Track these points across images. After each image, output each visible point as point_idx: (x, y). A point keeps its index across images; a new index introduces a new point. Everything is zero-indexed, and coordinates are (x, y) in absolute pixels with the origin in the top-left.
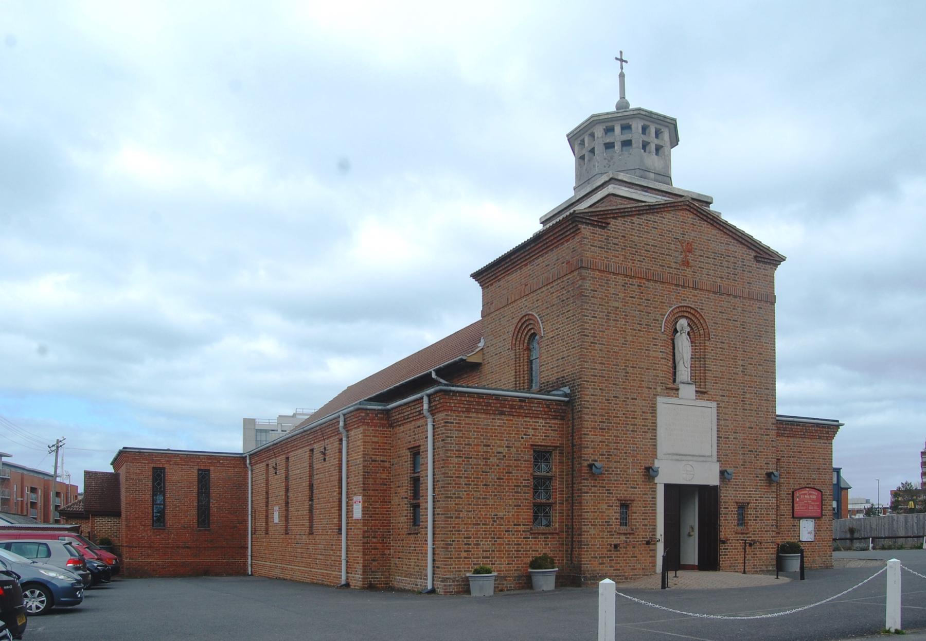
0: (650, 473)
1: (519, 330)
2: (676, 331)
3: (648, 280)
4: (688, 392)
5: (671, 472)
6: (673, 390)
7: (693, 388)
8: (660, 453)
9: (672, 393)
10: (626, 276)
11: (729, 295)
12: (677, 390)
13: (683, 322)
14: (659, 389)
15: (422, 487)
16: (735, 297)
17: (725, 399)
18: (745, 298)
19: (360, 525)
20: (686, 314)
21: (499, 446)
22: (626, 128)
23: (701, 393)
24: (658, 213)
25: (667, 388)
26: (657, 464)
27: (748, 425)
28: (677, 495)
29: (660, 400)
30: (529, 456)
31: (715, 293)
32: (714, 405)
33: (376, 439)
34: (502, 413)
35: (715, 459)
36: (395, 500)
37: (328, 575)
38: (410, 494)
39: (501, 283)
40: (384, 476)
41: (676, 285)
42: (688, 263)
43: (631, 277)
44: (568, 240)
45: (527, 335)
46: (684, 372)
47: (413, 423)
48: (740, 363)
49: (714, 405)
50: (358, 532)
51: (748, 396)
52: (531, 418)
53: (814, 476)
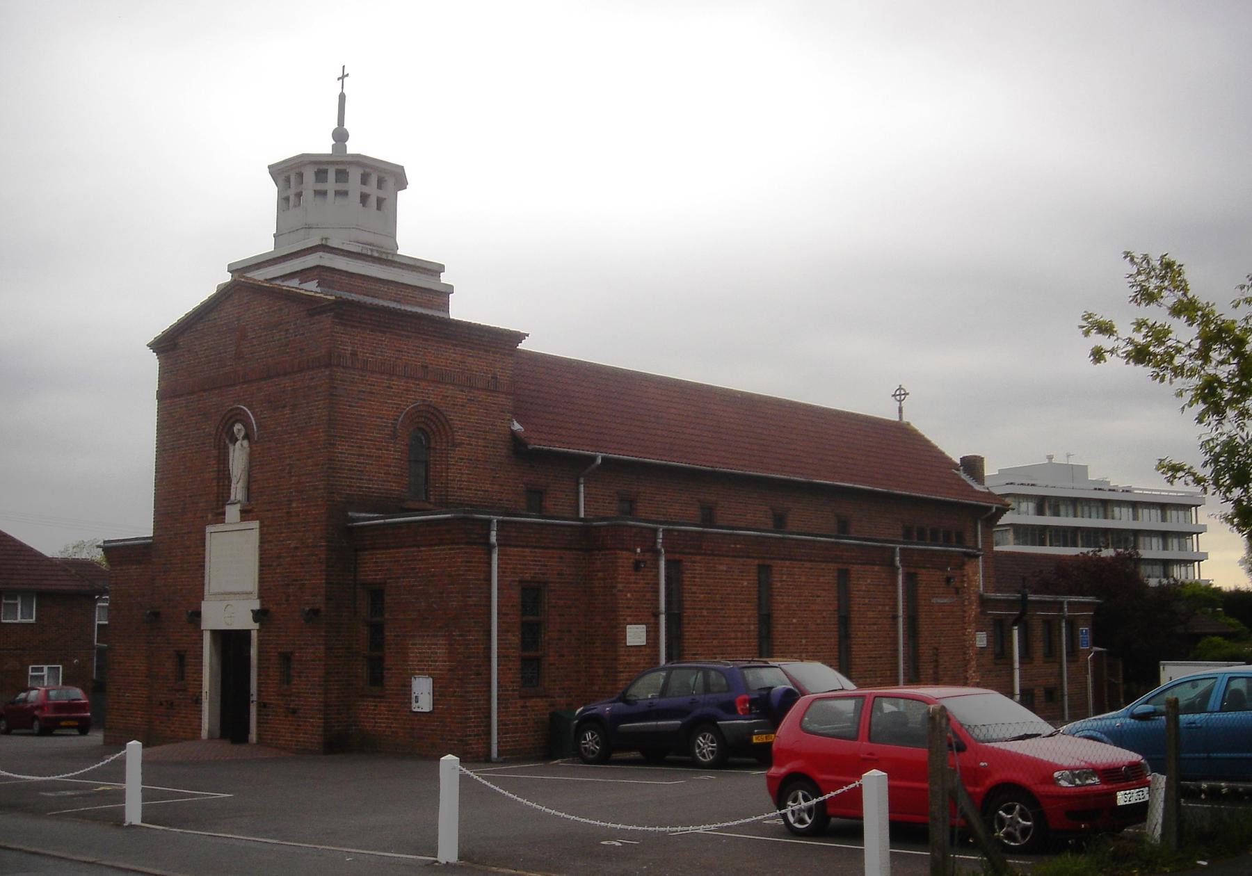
0: (197, 615)
6: (220, 517)
14: (210, 516)
23: (246, 514)
29: (209, 529)
32: (256, 524)
35: (256, 595)
46: (237, 491)
49: (256, 524)
51: (294, 505)
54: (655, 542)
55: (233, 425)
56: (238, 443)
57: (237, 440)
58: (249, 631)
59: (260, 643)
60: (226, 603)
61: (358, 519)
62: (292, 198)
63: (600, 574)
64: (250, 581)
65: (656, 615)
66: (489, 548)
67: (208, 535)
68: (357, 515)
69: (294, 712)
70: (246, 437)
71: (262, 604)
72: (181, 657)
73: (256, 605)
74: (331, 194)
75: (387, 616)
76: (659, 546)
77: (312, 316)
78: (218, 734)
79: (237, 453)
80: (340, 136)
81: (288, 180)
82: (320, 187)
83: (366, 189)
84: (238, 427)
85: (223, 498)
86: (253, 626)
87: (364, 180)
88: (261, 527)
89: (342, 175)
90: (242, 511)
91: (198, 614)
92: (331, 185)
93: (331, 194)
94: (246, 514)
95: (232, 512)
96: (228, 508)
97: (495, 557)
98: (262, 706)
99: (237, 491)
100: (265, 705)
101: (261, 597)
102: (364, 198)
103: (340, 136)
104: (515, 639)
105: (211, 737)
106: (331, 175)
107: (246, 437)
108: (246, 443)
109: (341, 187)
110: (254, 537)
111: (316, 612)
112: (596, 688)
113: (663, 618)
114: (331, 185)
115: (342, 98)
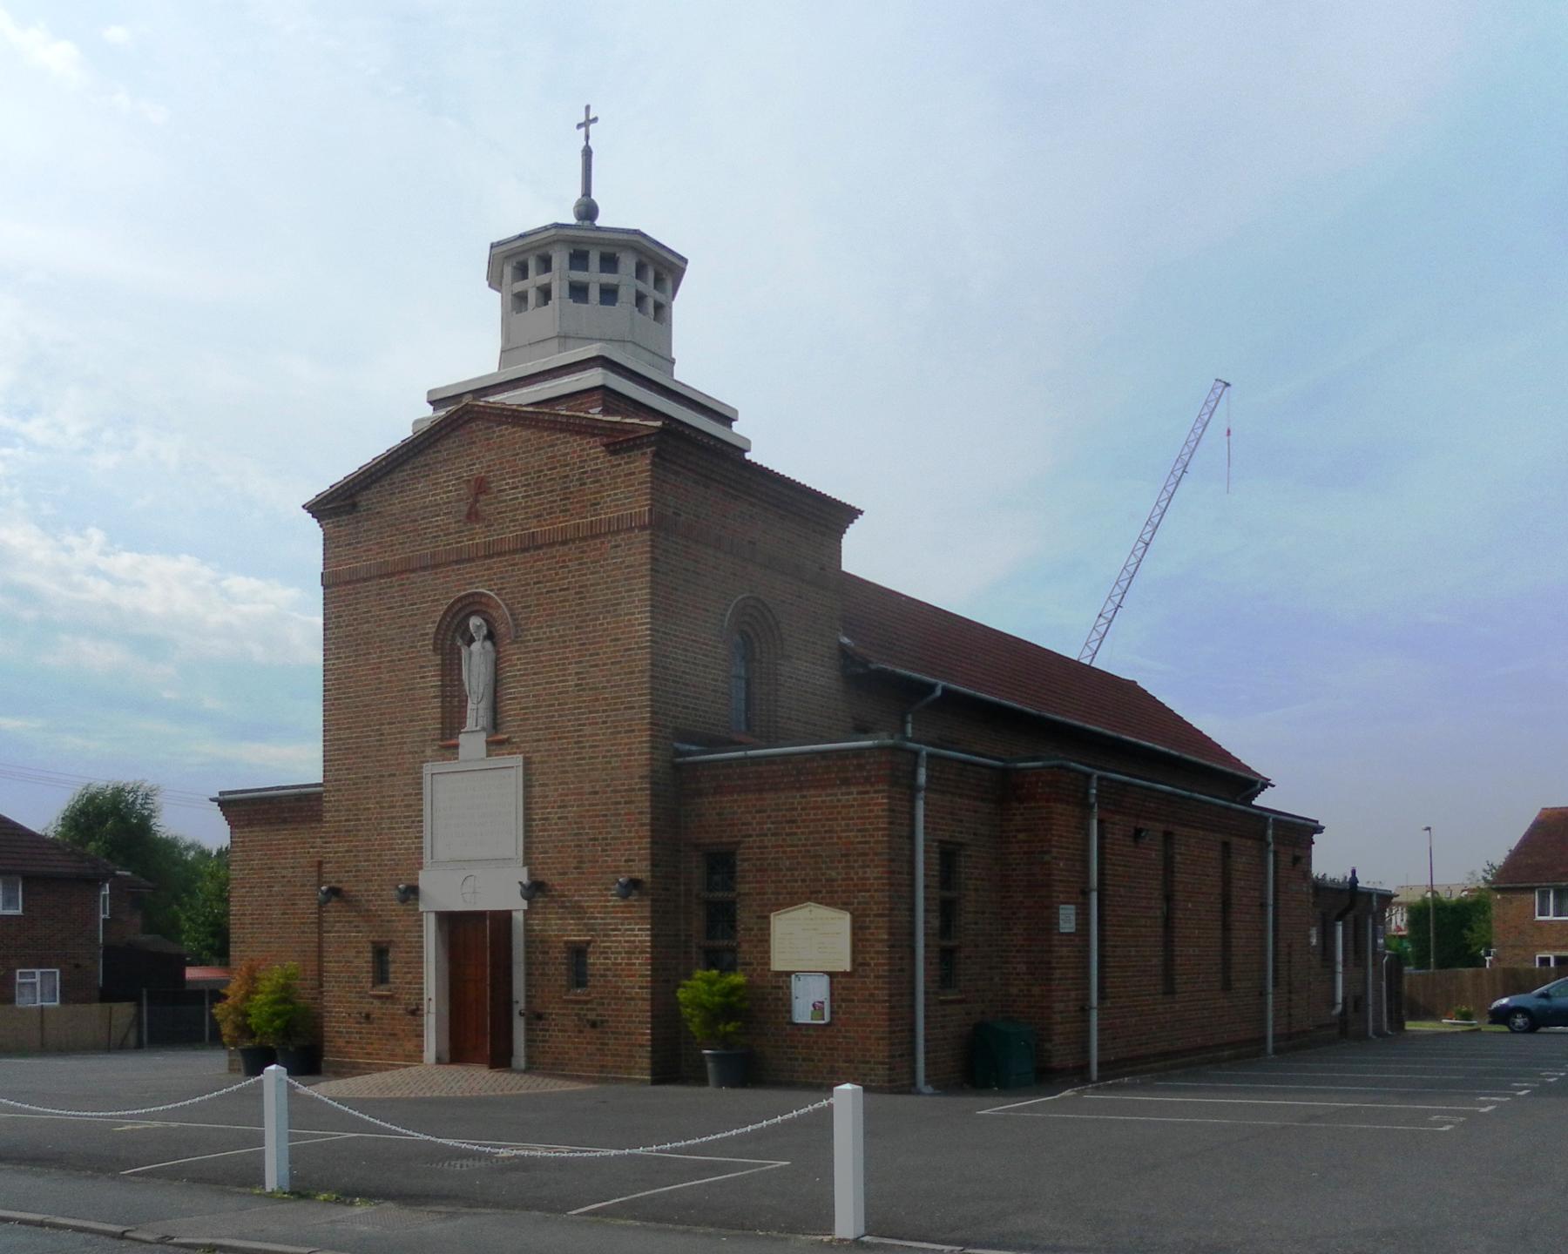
0: (412, 892)
3: (413, 571)
5: (443, 890)
6: (449, 749)
7: (483, 736)
9: (448, 754)
11: (552, 544)
12: (456, 746)
14: (429, 752)
16: (564, 543)
18: (584, 539)
20: (477, 607)
22: (546, 264)
23: (496, 745)
24: (429, 447)
25: (443, 747)
27: (587, 787)
28: (455, 924)
29: (428, 769)
42: (477, 514)
46: (476, 712)
51: (588, 730)
53: (834, 874)
54: (1087, 794)
56: (476, 646)
57: (471, 640)
58: (507, 916)
59: (528, 930)
61: (690, 753)
62: (532, 297)
63: (1021, 836)
64: (512, 842)
65: (1085, 893)
66: (913, 789)
67: (427, 780)
68: (687, 747)
69: (594, 1025)
70: (490, 636)
71: (530, 874)
72: (381, 953)
73: (523, 875)
74: (594, 293)
75: (743, 888)
76: (1093, 800)
78: (447, 1057)
79: (476, 659)
80: (588, 210)
81: (522, 271)
82: (579, 276)
83: (641, 286)
84: (475, 622)
85: (452, 722)
86: (524, 905)
87: (640, 271)
88: (527, 763)
89: (609, 263)
90: (488, 743)
92: (594, 277)
93: (594, 293)
95: (472, 743)
96: (462, 739)
97: (920, 805)
98: (535, 1017)
99: (476, 712)
100: (540, 1017)
101: (528, 860)
102: (640, 299)
103: (588, 210)
104: (936, 923)
105: (439, 1061)
107: (490, 636)
108: (488, 644)
109: (608, 278)
110: (515, 778)
111: (634, 884)
112: (1014, 991)
113: (1094, 896)
114: (594, 277)
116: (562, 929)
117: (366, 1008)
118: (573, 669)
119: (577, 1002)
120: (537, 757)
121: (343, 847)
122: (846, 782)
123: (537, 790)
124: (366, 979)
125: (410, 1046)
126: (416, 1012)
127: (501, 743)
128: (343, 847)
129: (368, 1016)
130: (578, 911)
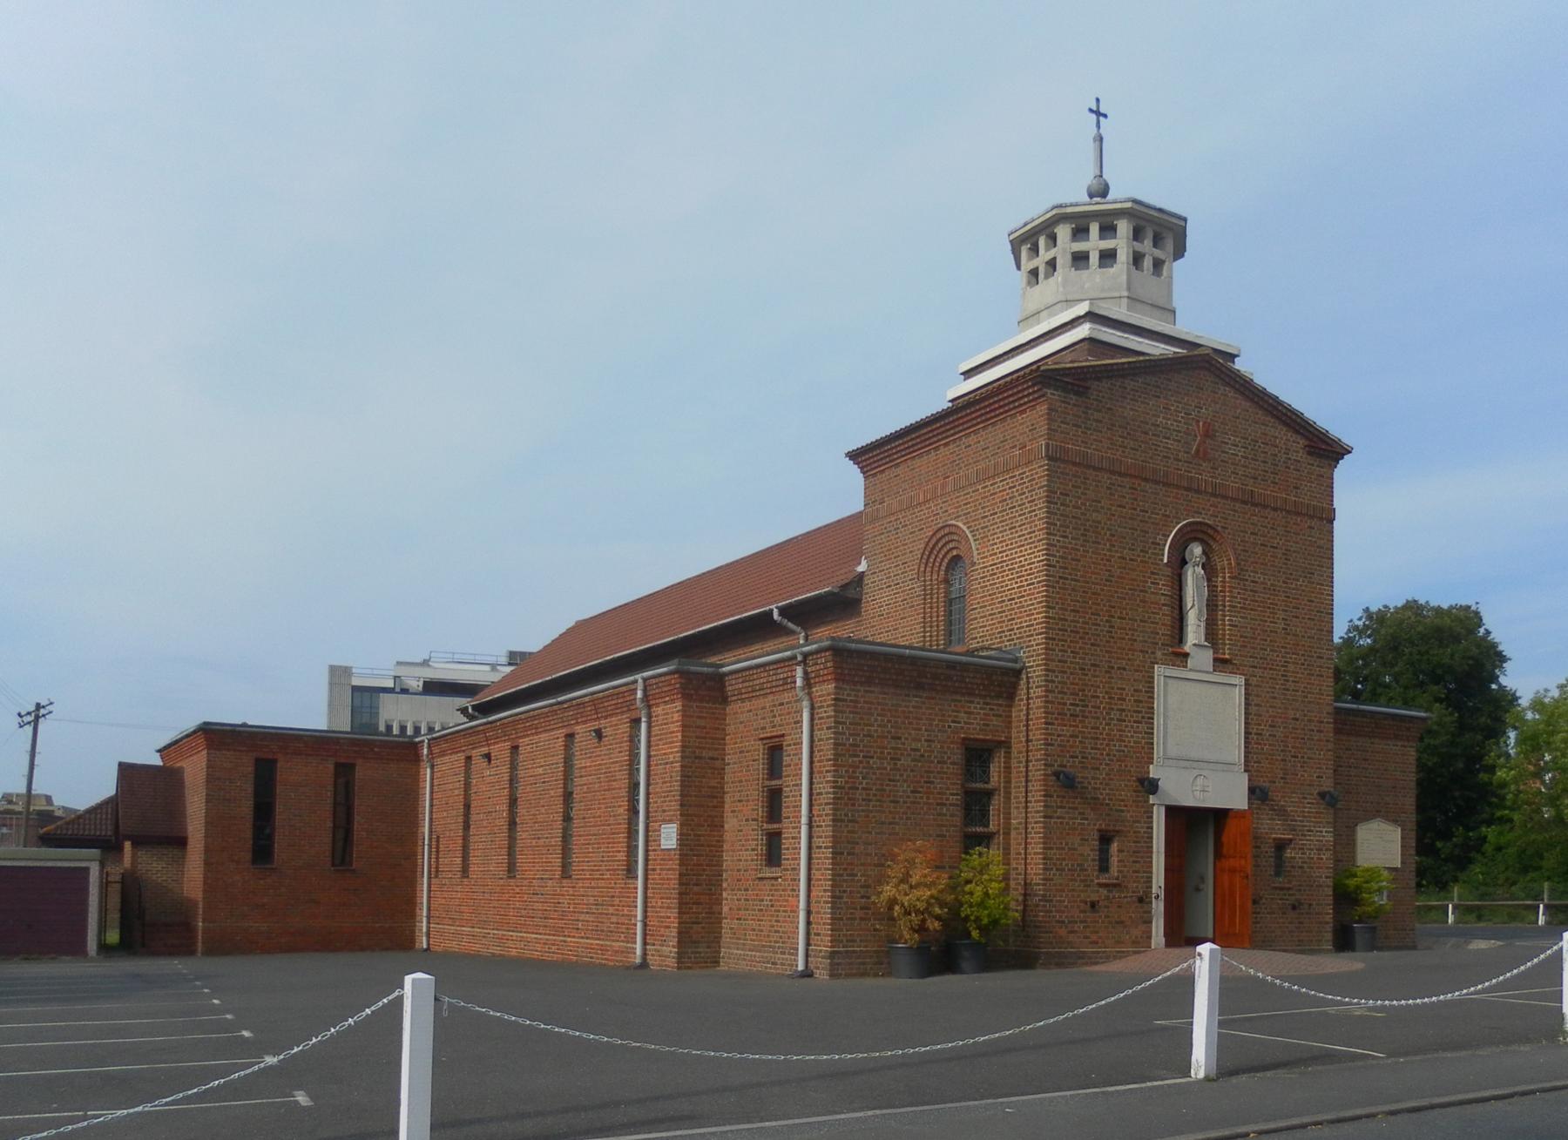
1: (931, 550)
2: (1184, 562)
3: (1146, 480)
4: (1202, 659)
8: (1158, 752)
10: (1113, 472)
11: (1265, 507)
13: (1197, 550)
14: (1159, 654)
15: (787, 802)
16: (1275, 509)
17: (1258, 672)
19: (675, 865)
21: (914, 740)
23: (1221, 663)
26: (1154, 772)
27: (1291, 714)
29: (1159, 671)
30: (957, 755)
31: (1245, 502)
33: (700, 722)
34: (920, 686)
36: (731, 823)
37: (604, 949)
38: (761, 812)
39: (899, 471)
40: (713, 783)
41: (1188, 489)
42: (1205, 453)
43: (1120, 474)
44: (1024, 412)
45: (947, 560)
47: (771, 697)
48: (1281, 615)
49: (1239, 680)
50: (669, 876)
51: (1291, 667)
52: (963, 695)
55: (1195, 539)
60: (1196, 772)
64: (1237, 754)
77: (1309, 453)
88: (1247, 684)
90: (1215, 660)
91: (1152, 786)
94: (1221, 663)
106: (1094, 229)
110: (1238, 695)
115: (1100, 139)
116: (1270, 827)
117: (1094, 897)
118: (1281, 615)
119: (1282, 889)
120: (1254, 681)
121: (1067, 731)
122: (1397, 737)
123: (1253, 709)
124: (1091, 865)
125: (1136, 932)
126: (1144, 900)
127: (1225, 661)
128: (1067, 731)
129: (1093, 905)
130: (1282, 813)
